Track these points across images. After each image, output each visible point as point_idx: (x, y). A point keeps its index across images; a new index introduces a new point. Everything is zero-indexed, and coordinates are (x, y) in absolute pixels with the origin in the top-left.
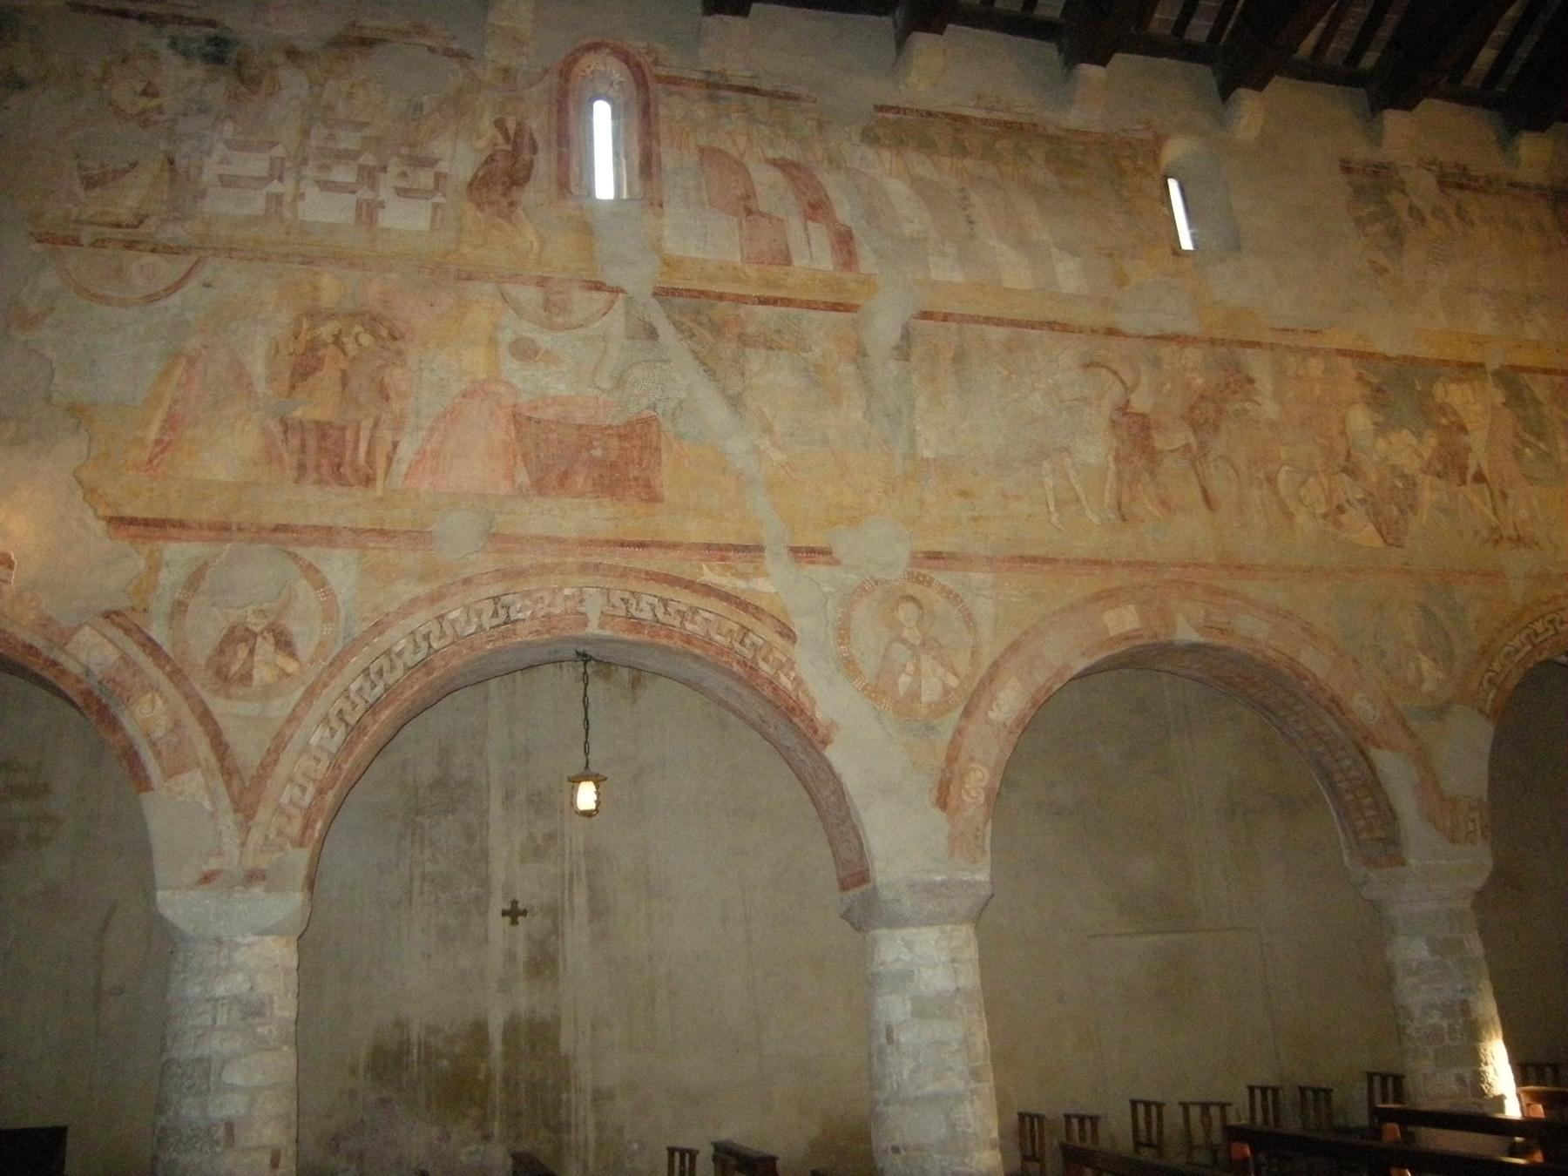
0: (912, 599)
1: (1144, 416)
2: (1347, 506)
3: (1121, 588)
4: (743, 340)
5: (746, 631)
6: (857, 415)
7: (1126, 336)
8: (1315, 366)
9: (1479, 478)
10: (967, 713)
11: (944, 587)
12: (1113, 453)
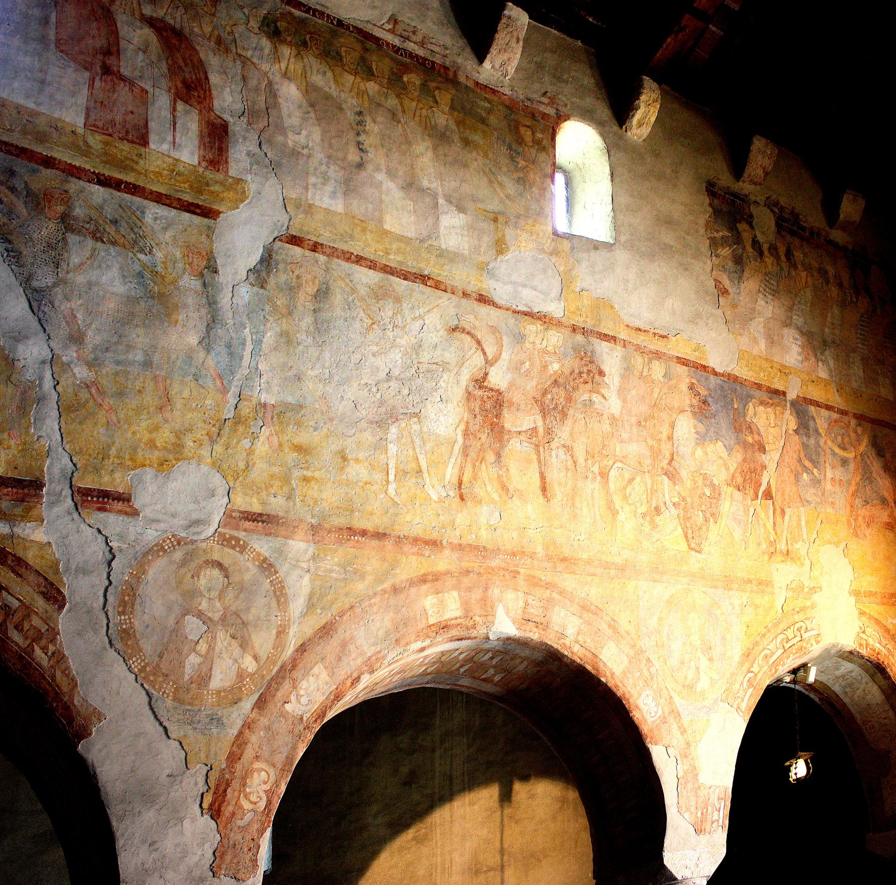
0: (219, 565)
2: (663, 509)
3: (448, 573)
6: (193, 339)
8: (658, 370)
9: (768, 495)
10: (261, 704)
11: (259, 554)
12: (462, 427)
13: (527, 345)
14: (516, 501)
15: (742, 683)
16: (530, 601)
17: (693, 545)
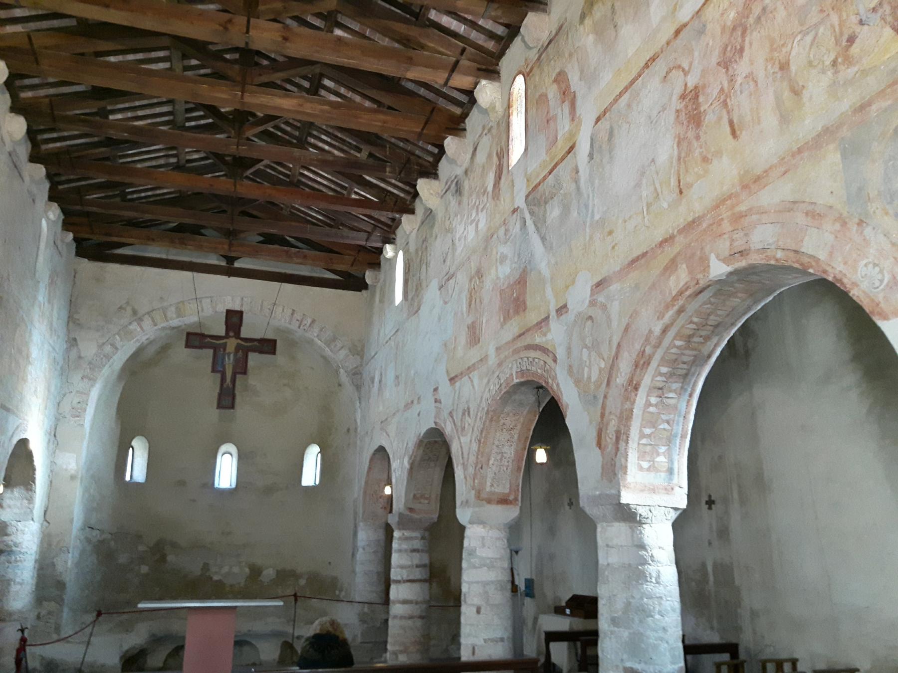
1: (696, 87)
3: (678, 253)
4: (546, 203)
7: (685, 25)
13: (709, 26)
14: (715, 162)
16: (734, 237)
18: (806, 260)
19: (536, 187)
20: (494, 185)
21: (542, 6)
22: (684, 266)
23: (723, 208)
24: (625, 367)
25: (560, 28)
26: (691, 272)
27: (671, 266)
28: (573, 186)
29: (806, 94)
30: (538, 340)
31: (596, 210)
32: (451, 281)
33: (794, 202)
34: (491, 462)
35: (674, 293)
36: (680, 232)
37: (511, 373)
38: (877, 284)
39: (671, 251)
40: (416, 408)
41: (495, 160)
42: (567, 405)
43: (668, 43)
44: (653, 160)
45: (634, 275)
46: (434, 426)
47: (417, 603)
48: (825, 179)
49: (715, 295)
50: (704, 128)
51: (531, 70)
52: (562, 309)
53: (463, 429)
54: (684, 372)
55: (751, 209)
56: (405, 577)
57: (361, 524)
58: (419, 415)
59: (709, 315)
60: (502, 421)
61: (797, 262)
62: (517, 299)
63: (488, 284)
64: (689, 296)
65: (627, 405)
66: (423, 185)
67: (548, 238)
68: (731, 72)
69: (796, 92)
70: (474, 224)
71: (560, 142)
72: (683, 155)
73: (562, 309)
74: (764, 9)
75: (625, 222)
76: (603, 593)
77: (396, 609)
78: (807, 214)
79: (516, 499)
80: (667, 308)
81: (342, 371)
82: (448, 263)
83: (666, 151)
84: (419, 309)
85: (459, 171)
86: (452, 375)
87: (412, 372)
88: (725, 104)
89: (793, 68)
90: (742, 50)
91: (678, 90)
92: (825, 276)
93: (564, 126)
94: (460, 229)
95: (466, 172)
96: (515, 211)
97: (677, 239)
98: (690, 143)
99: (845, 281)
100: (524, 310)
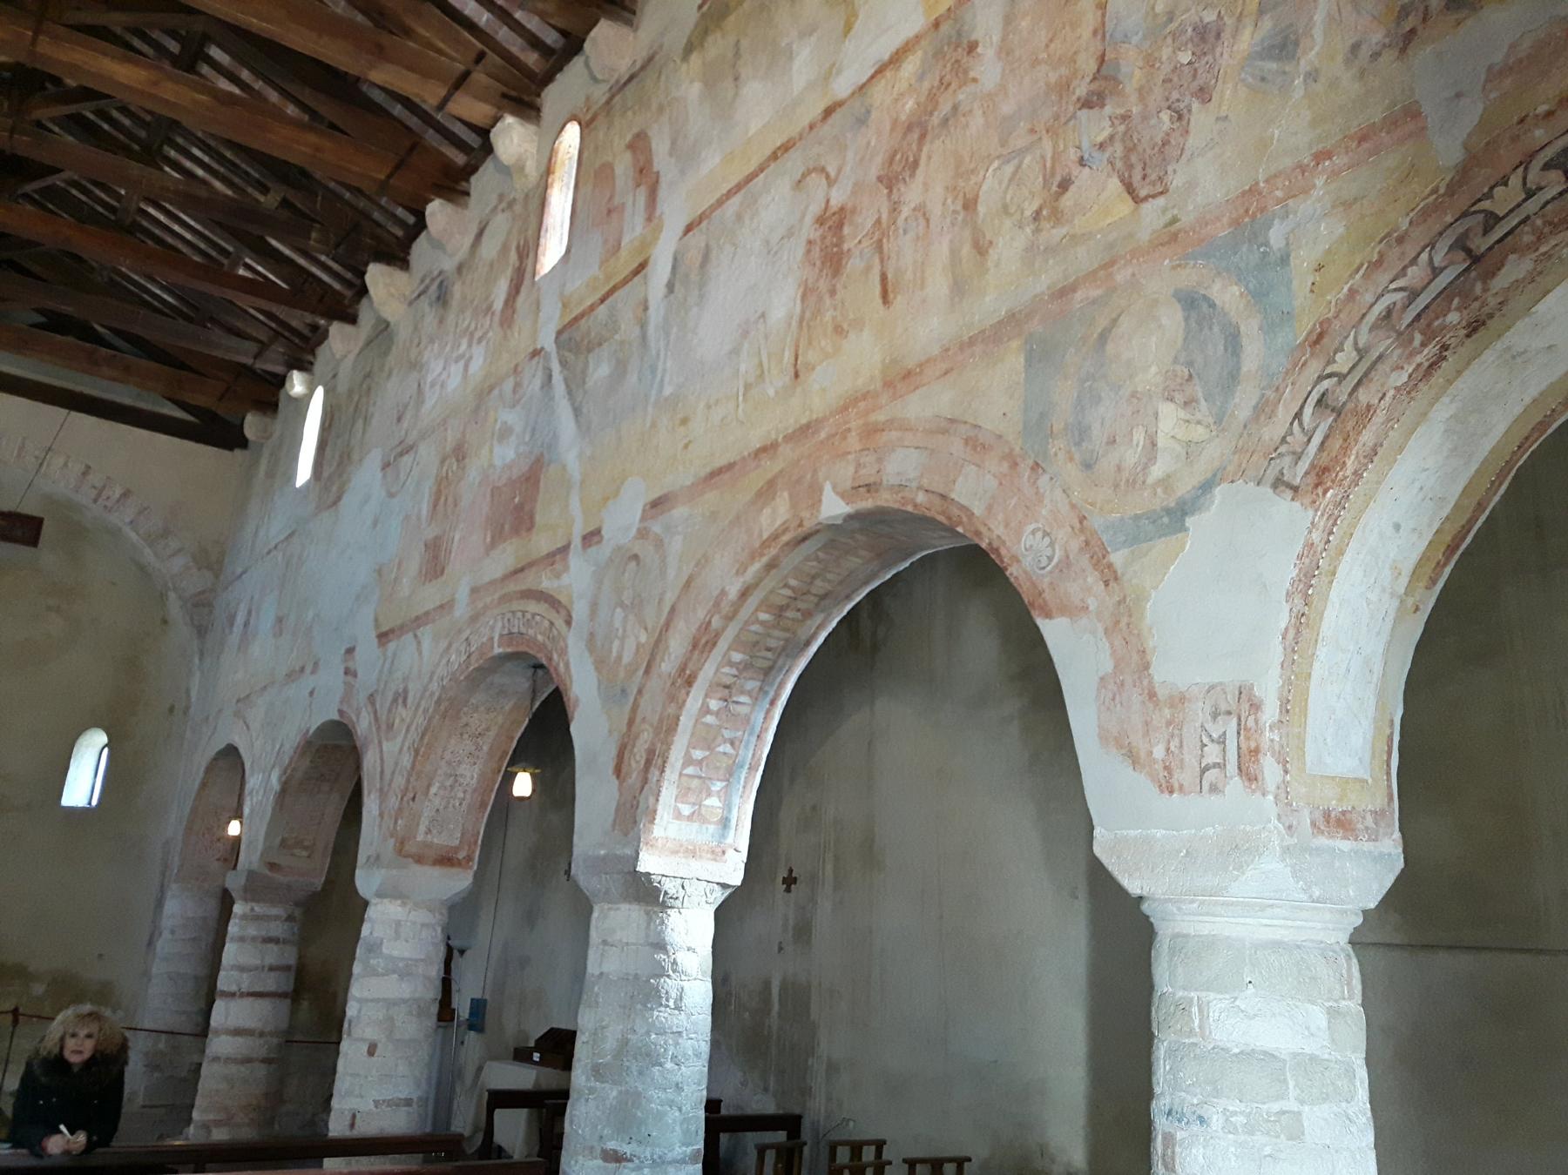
1: (842, 209)
4: (589, 351)
5: (552, 624)
7: (840, 104)
10: (647, 671)
13: (874, 115)
14: (852, 336)
15: (1298, 415)
17: (1143, 193)
18: (955, 511)
19: (576, 319)
20: (506, 303)
21: (627, 15)
22: (786, 494)
23: (853, 412)
24: (677, 645)
25: (650, 59)
26: (794, 505)
27: (767, 492)
28: (637, 331)
29: (993, 254)
30: (546, 583)
31: (667, 379)
32: (406, 458)
33: (952, 421)
34: (433, 790)
35: (765, 536)
36: (788, 438)
37: (492, 636)
38: (1044, 561)
39: (771, 467)
40: (308, 681)
41: (513, 256)
42: (577, 700)
43: (811, 127)
44: (763, 315)
45: (711, 497)
46: (336, 717)
47: (262, 1034)
48: (997, 393)
49: (824, 548)
50: (844, 278)
51: (593, 119)
52: (592, 537)
53: (390, 727)
54: (766, 664)
55: (891, 421)
56: (244, 989)
57: (174, 886)
58: (311, 693)
59: (814, 577)
60: (464, 720)
61: (943, 513)
62: (519, 508)
63: (473, 474)
64: (787, 544)
65: (671, 710)
66: (377, 276)
67: (585, 410)
68: (895, 197)
69: (981, 249)
70: (462, 363)
71: (624, 253)
72: (808, 315)
73: (592, 537)
74: (955, 108)
75: (709, 407)
76: (586, 1023)
77: (219, 1045)
78: (967, 441)
79: (469, 858)
80: (753, 557)
81: (172, 595)
82: (405, 424)
83: (783, 304)
84: (339, 498)
85: (448, 265)
86: (384, 629)
87: (311, 614)
88: (879, 246)
89: (981, 209)
90: (916, 164)
91: (815, 209)
92: (976, 541)
93: (634, 228)
94: (436, 367)
95: (460, 269)
96: (536, 353)
97: (781, 449)
98: (820, 299)
99: (1003, 551)
100: (530, 529)
